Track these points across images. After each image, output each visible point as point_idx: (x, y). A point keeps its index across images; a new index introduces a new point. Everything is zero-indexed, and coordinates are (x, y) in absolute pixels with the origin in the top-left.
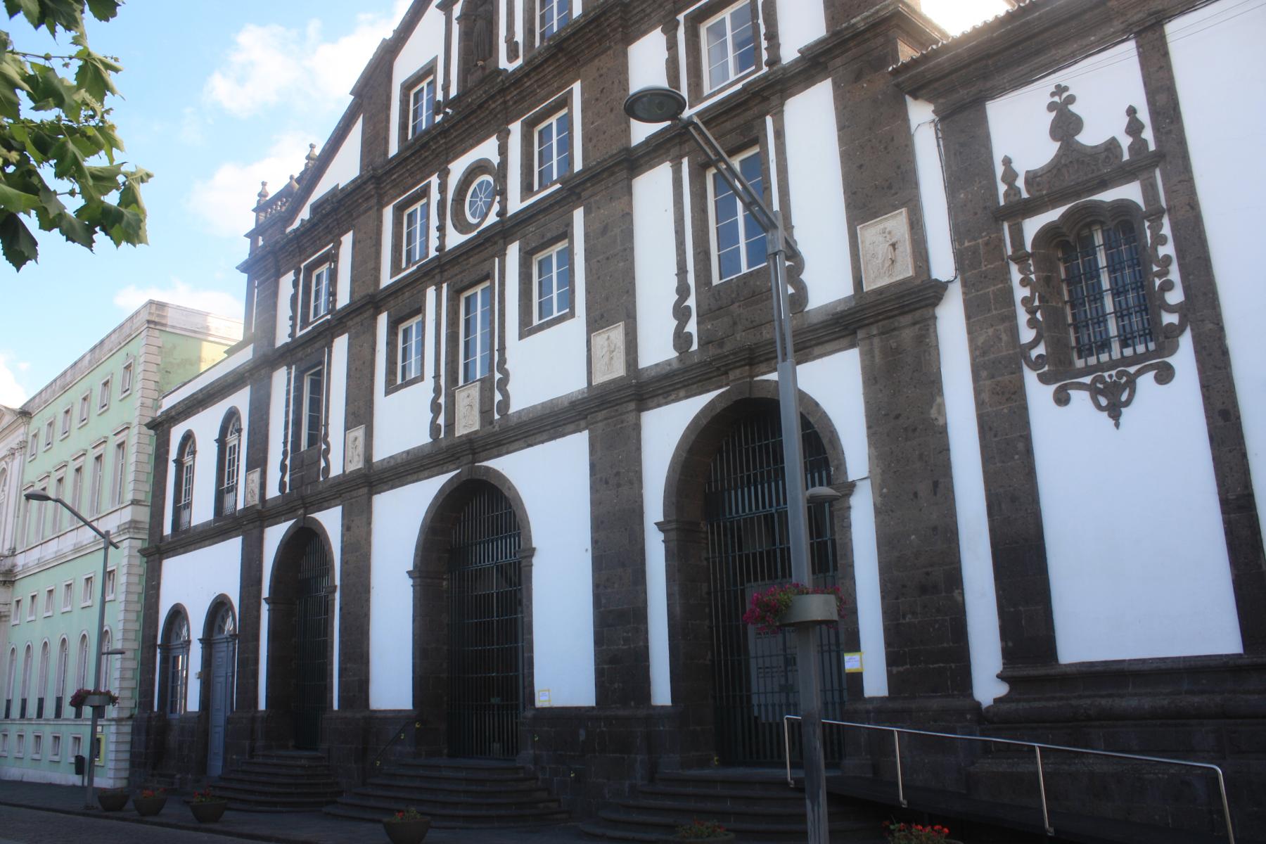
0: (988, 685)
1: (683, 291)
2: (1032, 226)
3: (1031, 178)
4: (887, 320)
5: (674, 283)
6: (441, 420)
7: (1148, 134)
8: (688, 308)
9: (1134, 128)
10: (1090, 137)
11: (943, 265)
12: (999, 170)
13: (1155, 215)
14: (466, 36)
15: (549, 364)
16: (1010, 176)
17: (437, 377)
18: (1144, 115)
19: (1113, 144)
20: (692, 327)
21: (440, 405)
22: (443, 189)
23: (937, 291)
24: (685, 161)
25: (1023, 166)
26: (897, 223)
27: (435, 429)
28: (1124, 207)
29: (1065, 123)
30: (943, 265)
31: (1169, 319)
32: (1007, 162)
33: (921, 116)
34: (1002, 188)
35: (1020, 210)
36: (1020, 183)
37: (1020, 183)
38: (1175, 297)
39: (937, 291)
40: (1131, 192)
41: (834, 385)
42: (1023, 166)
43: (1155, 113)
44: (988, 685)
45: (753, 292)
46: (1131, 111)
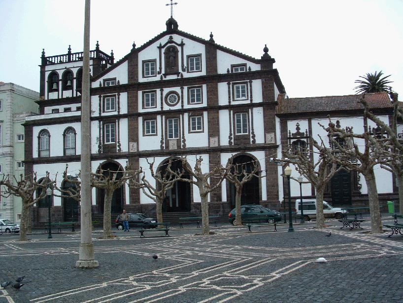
0: (281, 199)
1: (231, 134)
2: (292, 141)
3: (292, 134)
4: (269, 149)
6: (164, 145)
7: (308, 133)
8: (232, 138)
9: (306, 132)
10: (301, 131)
11: (279, 142)
12: (288, 132)
13: (308, 144)
14: (167, 58)
15: (197, 140)
16: (290, 133)
17: (162, 136)
19: (303, 133)
20: (232, 141)
23: (278, 146)
24: (232, 111)
25: (292, 132)
26: (273, 135)
28: (304, 142)
29: (298, 129)
30: (279, 142)
31: (308, 157)
33: (277, 120)
34: (288, 134)
35: (290, 138)
38: (309, 154)
39: (278, 146)
40: (305, 140)
41: (260, 156)
42: (292, 132)
44: (281, 199)
45: (246, 138)
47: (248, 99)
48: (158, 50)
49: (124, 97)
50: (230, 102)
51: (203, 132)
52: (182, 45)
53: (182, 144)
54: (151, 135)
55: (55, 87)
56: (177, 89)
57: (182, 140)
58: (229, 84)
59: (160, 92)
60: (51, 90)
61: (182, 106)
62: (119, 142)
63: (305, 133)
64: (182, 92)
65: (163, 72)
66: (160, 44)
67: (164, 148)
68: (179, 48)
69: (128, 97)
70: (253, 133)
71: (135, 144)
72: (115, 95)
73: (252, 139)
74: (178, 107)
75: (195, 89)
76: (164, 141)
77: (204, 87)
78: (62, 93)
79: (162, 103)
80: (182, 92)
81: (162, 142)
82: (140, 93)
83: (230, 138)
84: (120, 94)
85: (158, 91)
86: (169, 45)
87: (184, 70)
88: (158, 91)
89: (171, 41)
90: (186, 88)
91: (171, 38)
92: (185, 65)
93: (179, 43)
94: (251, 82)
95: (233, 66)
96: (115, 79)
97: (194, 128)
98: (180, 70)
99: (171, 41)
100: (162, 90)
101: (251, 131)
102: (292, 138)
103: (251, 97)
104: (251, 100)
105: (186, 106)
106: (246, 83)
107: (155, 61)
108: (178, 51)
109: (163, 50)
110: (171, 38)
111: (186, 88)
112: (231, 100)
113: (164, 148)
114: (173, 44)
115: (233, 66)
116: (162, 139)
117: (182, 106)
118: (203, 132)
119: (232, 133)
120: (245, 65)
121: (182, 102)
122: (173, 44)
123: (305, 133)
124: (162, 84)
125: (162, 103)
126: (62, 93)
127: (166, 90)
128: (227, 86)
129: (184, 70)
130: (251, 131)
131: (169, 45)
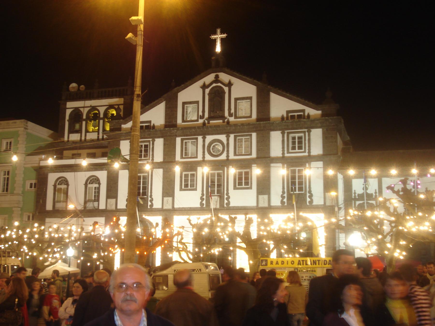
1: (283, 192)
3: (358, 195)
5: (282, 190)
6: (204, 202)
9: (376, 193)
10: (369, 191)
12: (353, 192)
16: (355, 193)
17: (203, 191)
18: (377, 191)
19: (372, 194)
20: (285, 200)
21: (204, 199)
22: (204, 141)
27: (202, 204)
28: (372, 204)
32: (355, 191)
34: (353, 195)
35: (355, 199)
36: (356, 195)
37: (356, 195)
43: (379, 191)
46: (376, 190)
47: (305, 152)
48: (201, 90)
49: (159, 143)
50: (283, 153)
51: (251, 188)
52: (230, 85)
53: (226, 201)
54: (190, 190)
55: (77, 126)
56: (223, 138)
57: (226, 197)
58: (283, 133)
59: (202, 140)
60: (72, 131)
61: (228, 156)
62: (151, 196)
63: (374, 194)
64: (228, 140)
65: (206, 115)
66: (204, 84)
67: (205, 206)
68: (226, 89)
69: (165, 144)
70: (310, 192)
71: (170, 199)
72: (149, 142)
73: (308, 200)
74: (223, 157)
75: (243, 138)
76: (205, 197)
77: (254, 135)
78: (86, 135)
79: (204, 152)
80: (228, 140)
81: (202, 199)
82: (178, 140)
83: (283, 197)
84: (155, 140)
85: (200, 138)
86: (214, 85)
87: (230, 115)
88: (200, 138)
89: (217, 80)
90: (232, 136)
91: (217, 77)
92: (233, 111)
93: (227, 81)
94: (309, 132)
95: (288, 112)
96: (150, 122)
97: (240, 184)
98: (226, 114)
99: (217, 80)
100: (204, 138)
101: (308, 190)
102: (358, 200)
103: (309, 149)
104: (309, 152)
105: (232, 156)
106: (304, 132)
107: (197, 102)
108: (224, 92)
109: (207, 91)
110: (217, 77)
111: (232, 136)
112: (286, 152)
113: (205, 206)
114: (219, 84)
115: (288, 112)
116: (203, 194)
117: (228, 156)
118: (251, 188)
119: (286, 190)
120: (303, 111)
121: (228, 151)
122: (219, 84)
123: (374, 194)
124: (204, 130)
125: (204, 152)
126: (86, 135)
127: (209, 138)
128: (281, 135)
129: (230, 115)
130: (308, 190)
131: (214, 85)
